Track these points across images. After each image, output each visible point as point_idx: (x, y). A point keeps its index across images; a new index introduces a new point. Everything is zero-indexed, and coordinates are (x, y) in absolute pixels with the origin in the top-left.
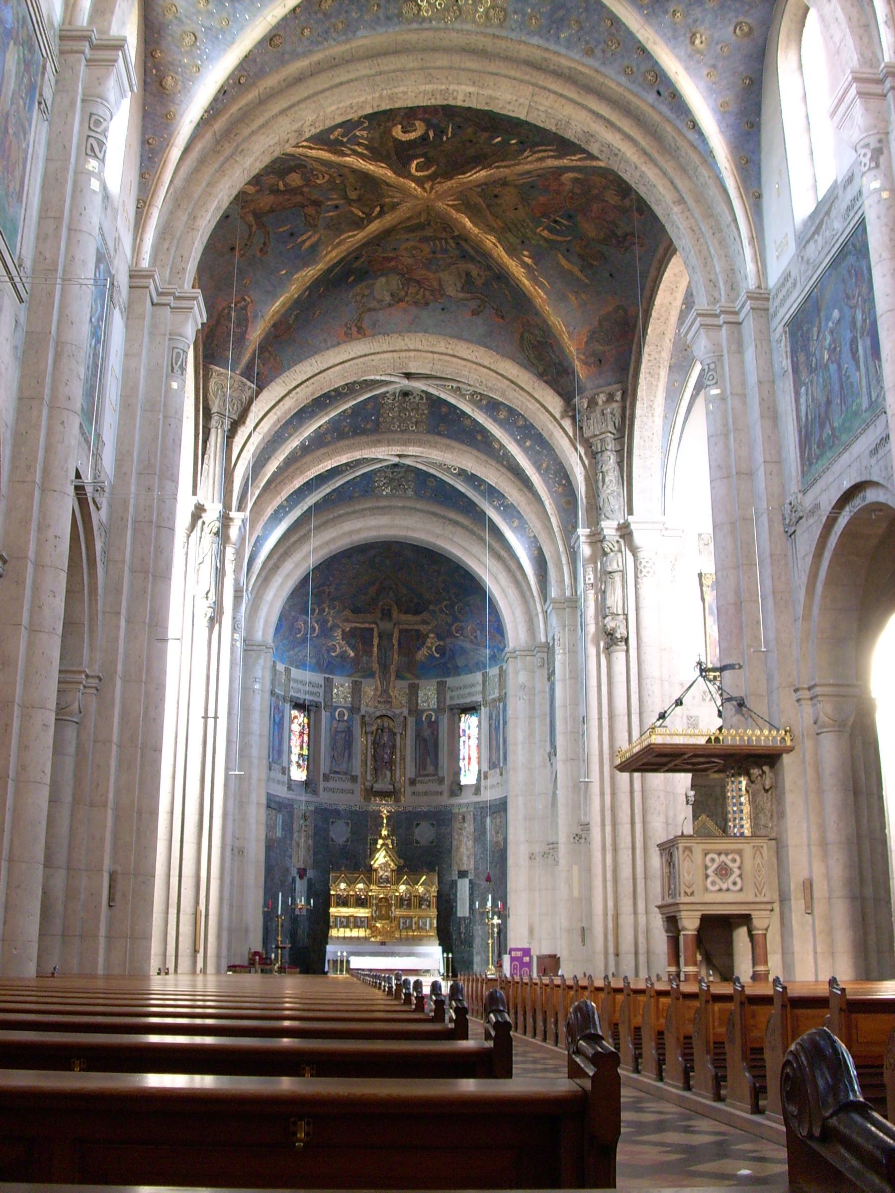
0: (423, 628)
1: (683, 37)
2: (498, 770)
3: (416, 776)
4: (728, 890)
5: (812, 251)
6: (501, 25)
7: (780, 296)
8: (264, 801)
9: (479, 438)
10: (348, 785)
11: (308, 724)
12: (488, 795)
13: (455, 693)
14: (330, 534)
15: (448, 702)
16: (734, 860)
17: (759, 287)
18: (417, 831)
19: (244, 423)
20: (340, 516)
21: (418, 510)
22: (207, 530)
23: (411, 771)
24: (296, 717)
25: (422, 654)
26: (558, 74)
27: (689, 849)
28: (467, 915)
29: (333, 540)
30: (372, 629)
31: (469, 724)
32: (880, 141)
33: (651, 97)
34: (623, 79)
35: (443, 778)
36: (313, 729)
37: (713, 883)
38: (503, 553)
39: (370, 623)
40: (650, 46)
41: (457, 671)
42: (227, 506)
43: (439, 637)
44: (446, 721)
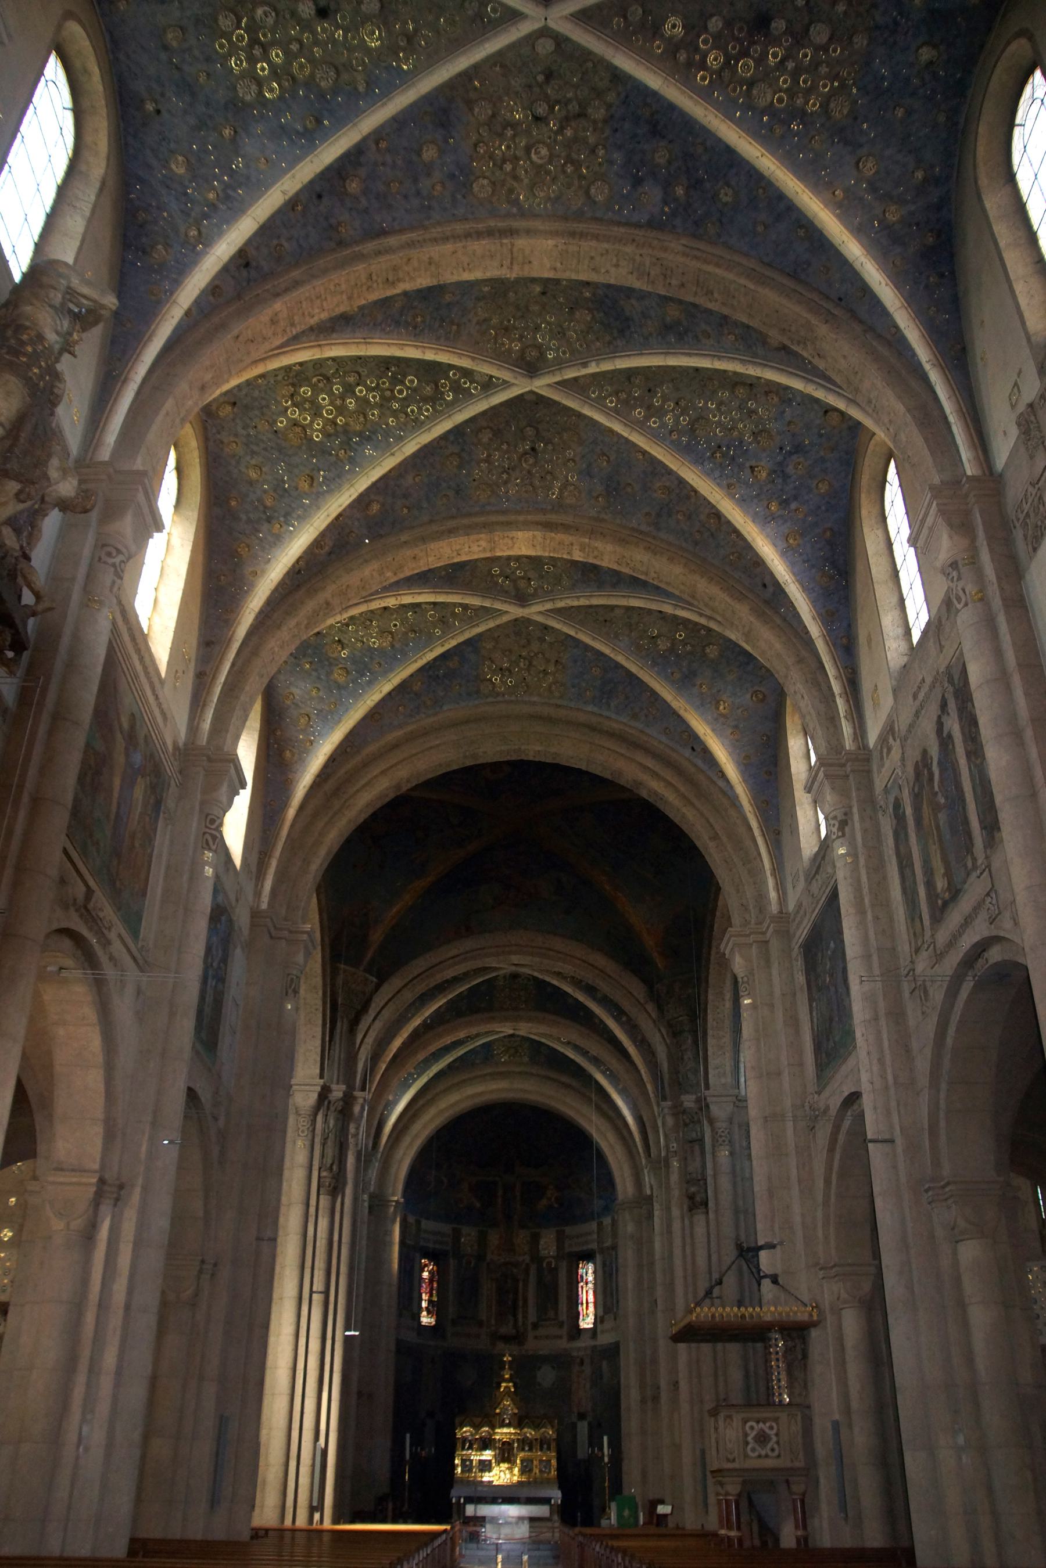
1: (707, 703)
4: (767, 1456)
5: (815, 887)
6: (561, 697)
7: (798, 920)
8: (393, 1347)
9: (582, 1014)
11: (438, 1271)
12: (605, 1339)
14: (454, 1097)
16: (771, 1428)
17: (781, 912)
19: (367, 1011)
20: (464, 1081)
21: (532, 1074)
22: (332, 1108)
23: (532, 1317)
24: (426, 1265)
26: (612, 735)
27: (730, 1417)
29: (456, 1103)
31: (588, 1272)
32: (845, 814)
33: (687, 752)
34: (664, 739)
36: (440, 1277)
37: (753, 1450)
38: (611, 1113)
40: (682, 712)
42: (351, 1087)
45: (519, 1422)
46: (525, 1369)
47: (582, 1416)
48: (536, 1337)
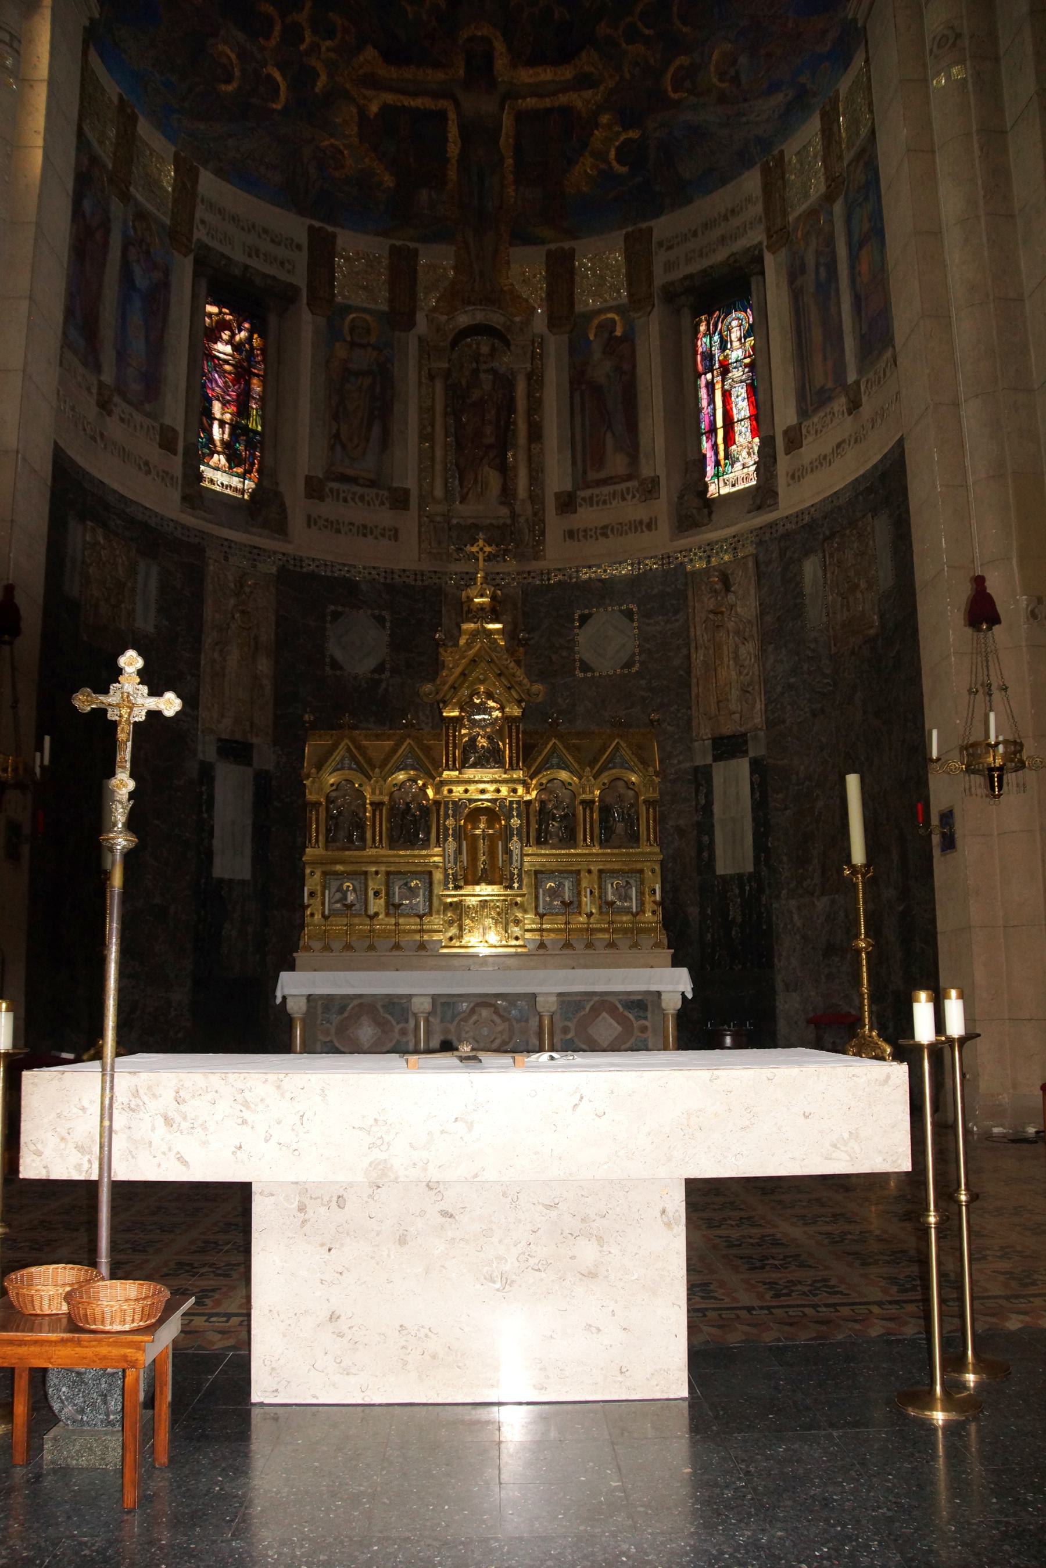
0: (579, 100)
2: (840, 404)
10: (384, 517)
12: (797, 498)
15: (660, 278)
18: (584, 637)
23: (557, 477)
24: (223, 325)
28: (750, 868)
30: (441, 116)
35: (655, 481)
41: (682, 193)
44: (654, 328)
45: (525, 745)
46: (545, 618)
47: (728, 747)
48: (571, 534)
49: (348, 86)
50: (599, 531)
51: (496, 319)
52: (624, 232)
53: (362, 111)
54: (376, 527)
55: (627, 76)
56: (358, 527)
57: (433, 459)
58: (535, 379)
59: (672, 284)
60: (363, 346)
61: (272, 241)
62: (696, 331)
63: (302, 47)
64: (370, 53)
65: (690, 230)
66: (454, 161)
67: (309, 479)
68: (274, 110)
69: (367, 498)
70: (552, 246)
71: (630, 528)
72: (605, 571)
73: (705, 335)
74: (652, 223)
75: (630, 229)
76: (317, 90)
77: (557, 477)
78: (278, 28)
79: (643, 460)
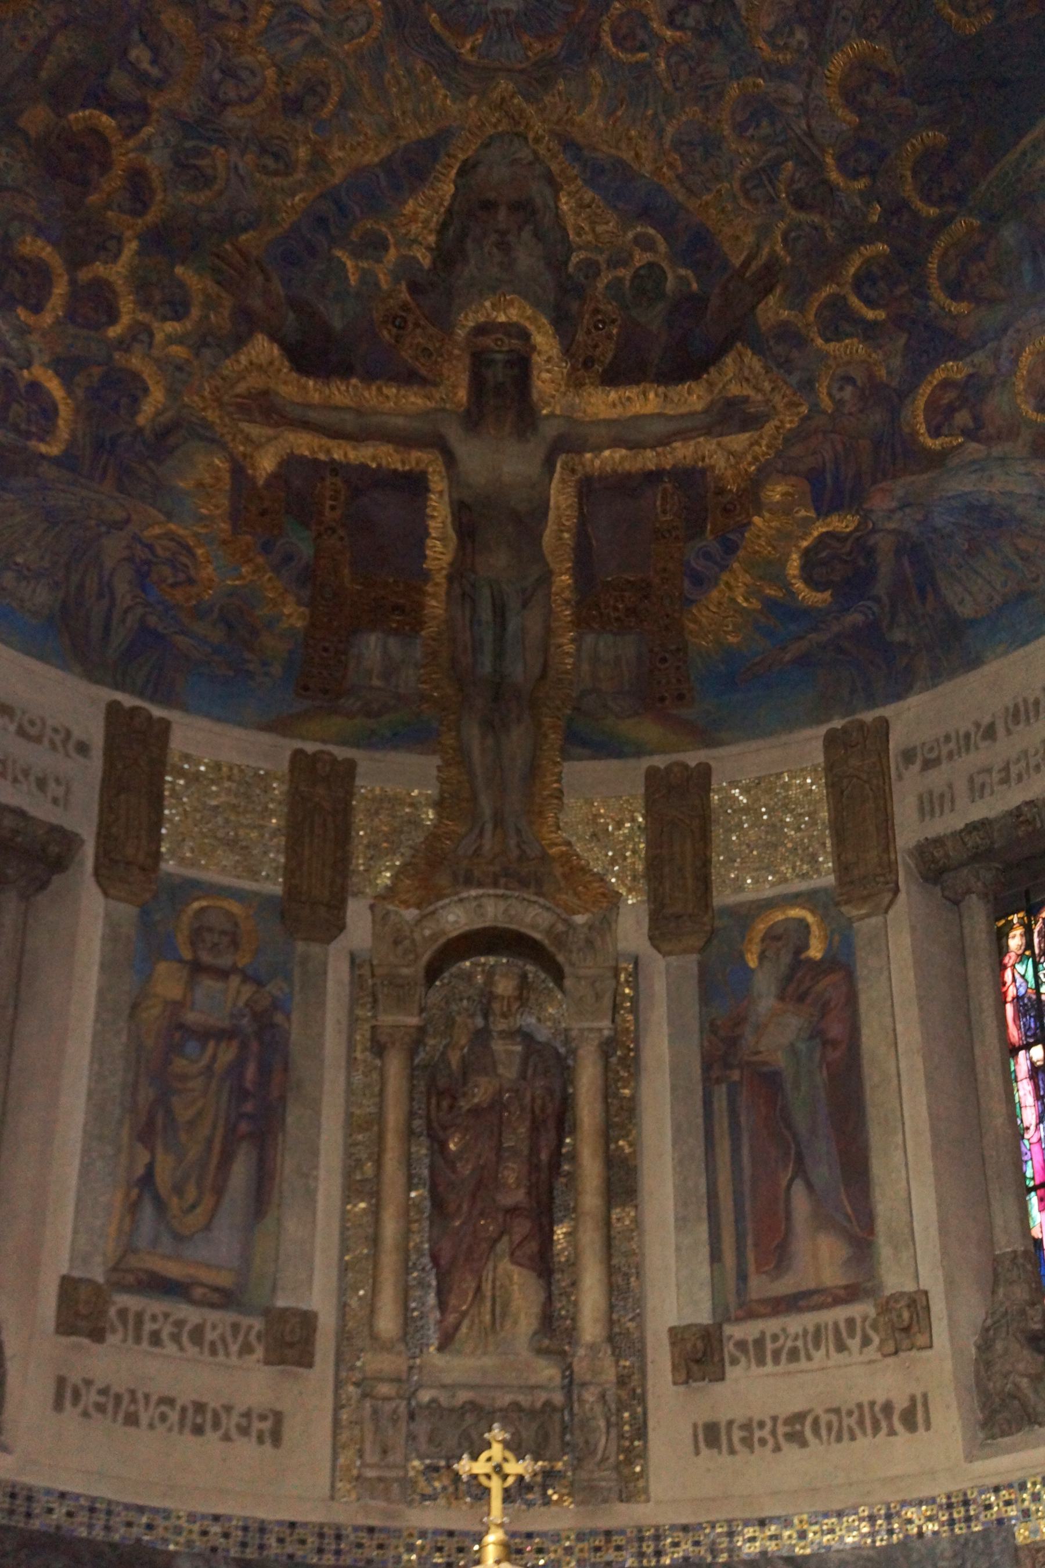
0: (723, 455)
3: (723, 1315)
10: (254, 1383)
13: (953, 774)
15: (910, 830)
23: (676, 1290)
25: (724, 609)
30: (414, 485)
35: (918, 1304)
39: (404, 441)
41: (954, 646)
43: (828, 493)
48: (711, 1435)
49: (211, 415)
50: (781, 1430)
51: (532, 917)
52: (823, 730)
53: (238, 470)
54: (228, 1409)
55: (827, 404)
56: (184, 1410)
57: (375, 1241)
58: (621, 1057)
59: (938, 841)
60: (223, 974)
61: (21, 732)
62: (1002, 949)
63: (113, 332)
64: (262, 348)
65: (978, 725)
66: (440, 578)
67: (68, 1286)
68: (42, 456)
69: (210, 1336)
70: (660, 761)
71: (861, 1423)
72: (802, 1535)
73: (1021, 958)
74: (887, 711)
75: (837, 723)
76: (141, 420)
77: (676, 1290)
78: (60, 289)
79: (885, 1251)
